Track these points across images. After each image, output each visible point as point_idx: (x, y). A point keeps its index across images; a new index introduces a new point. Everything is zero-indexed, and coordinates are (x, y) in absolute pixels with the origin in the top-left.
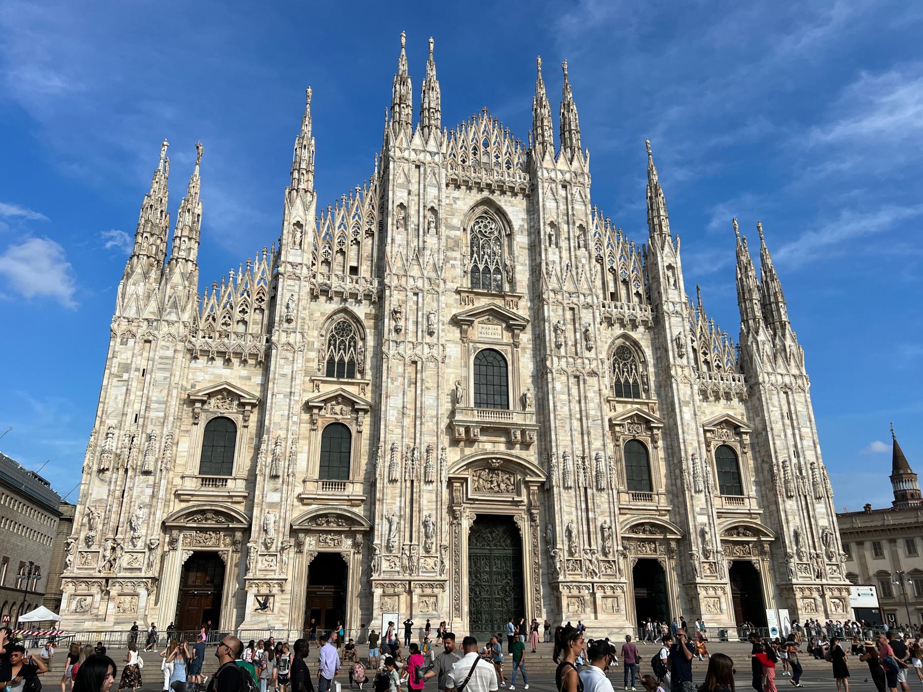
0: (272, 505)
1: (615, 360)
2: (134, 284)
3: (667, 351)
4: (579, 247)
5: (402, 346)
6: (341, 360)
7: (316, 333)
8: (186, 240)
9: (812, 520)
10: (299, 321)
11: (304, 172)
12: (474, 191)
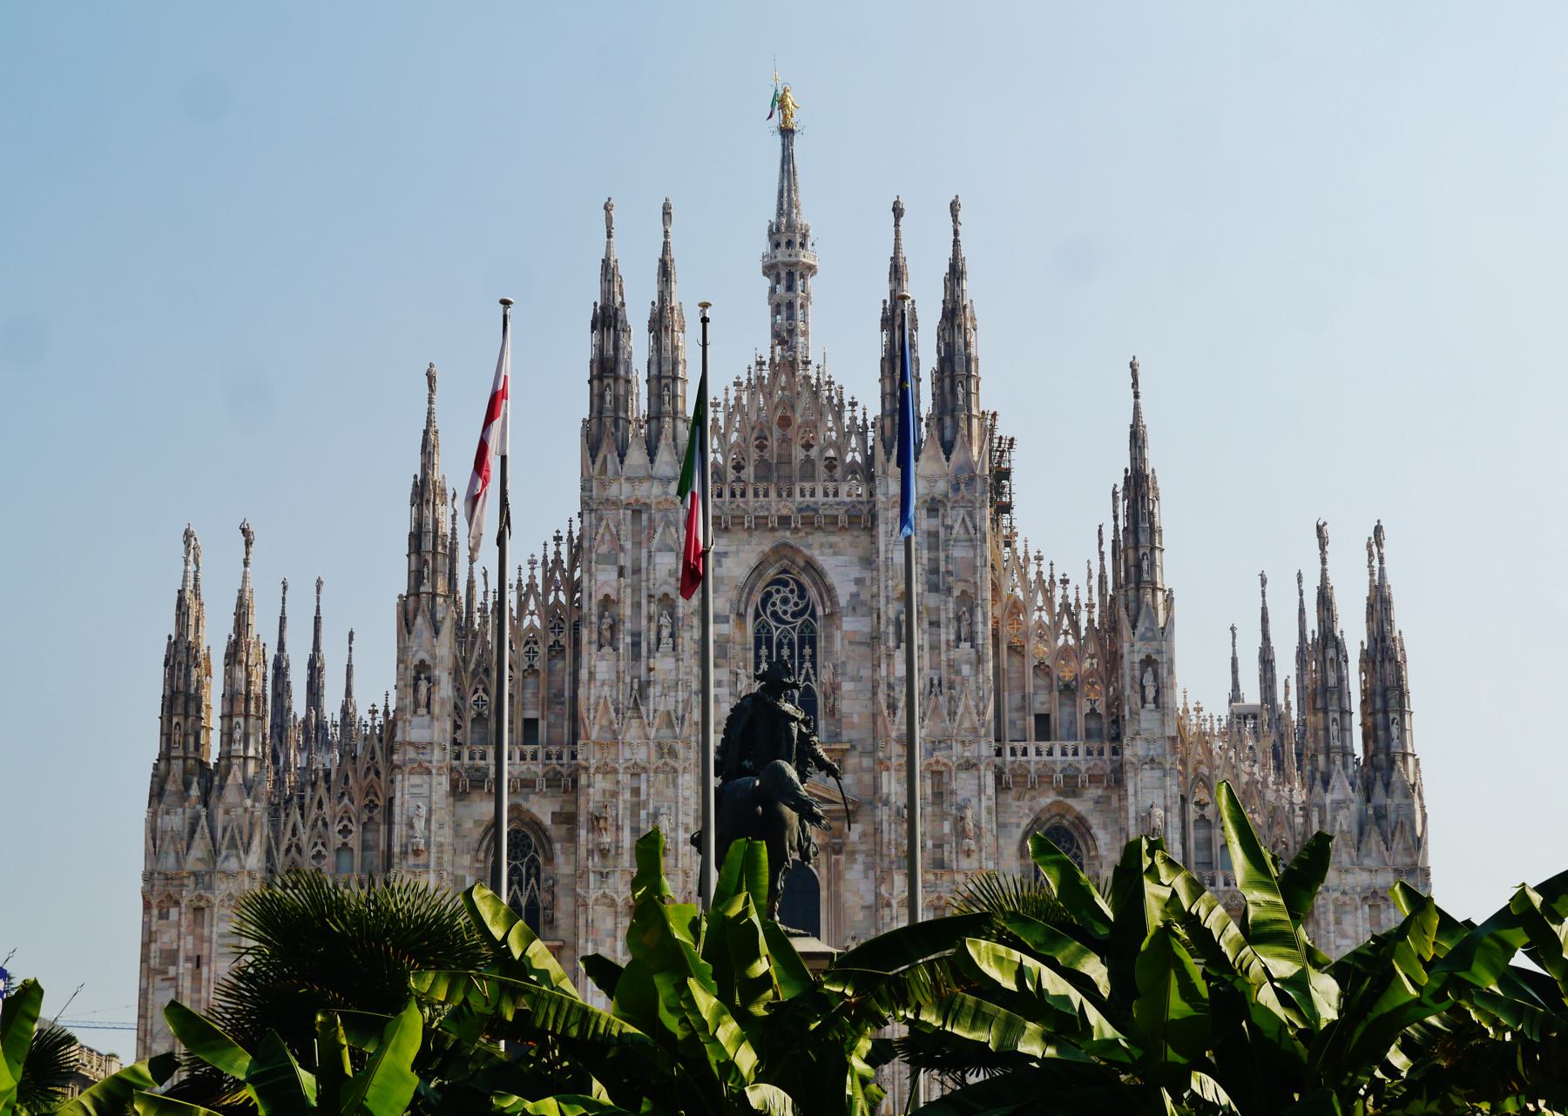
2: (168, 813)
4: (959, 638)
5: (611, 881)
7: (466, 860)
8: (241, 720)
10: (433, 850)
11: (429, 557)
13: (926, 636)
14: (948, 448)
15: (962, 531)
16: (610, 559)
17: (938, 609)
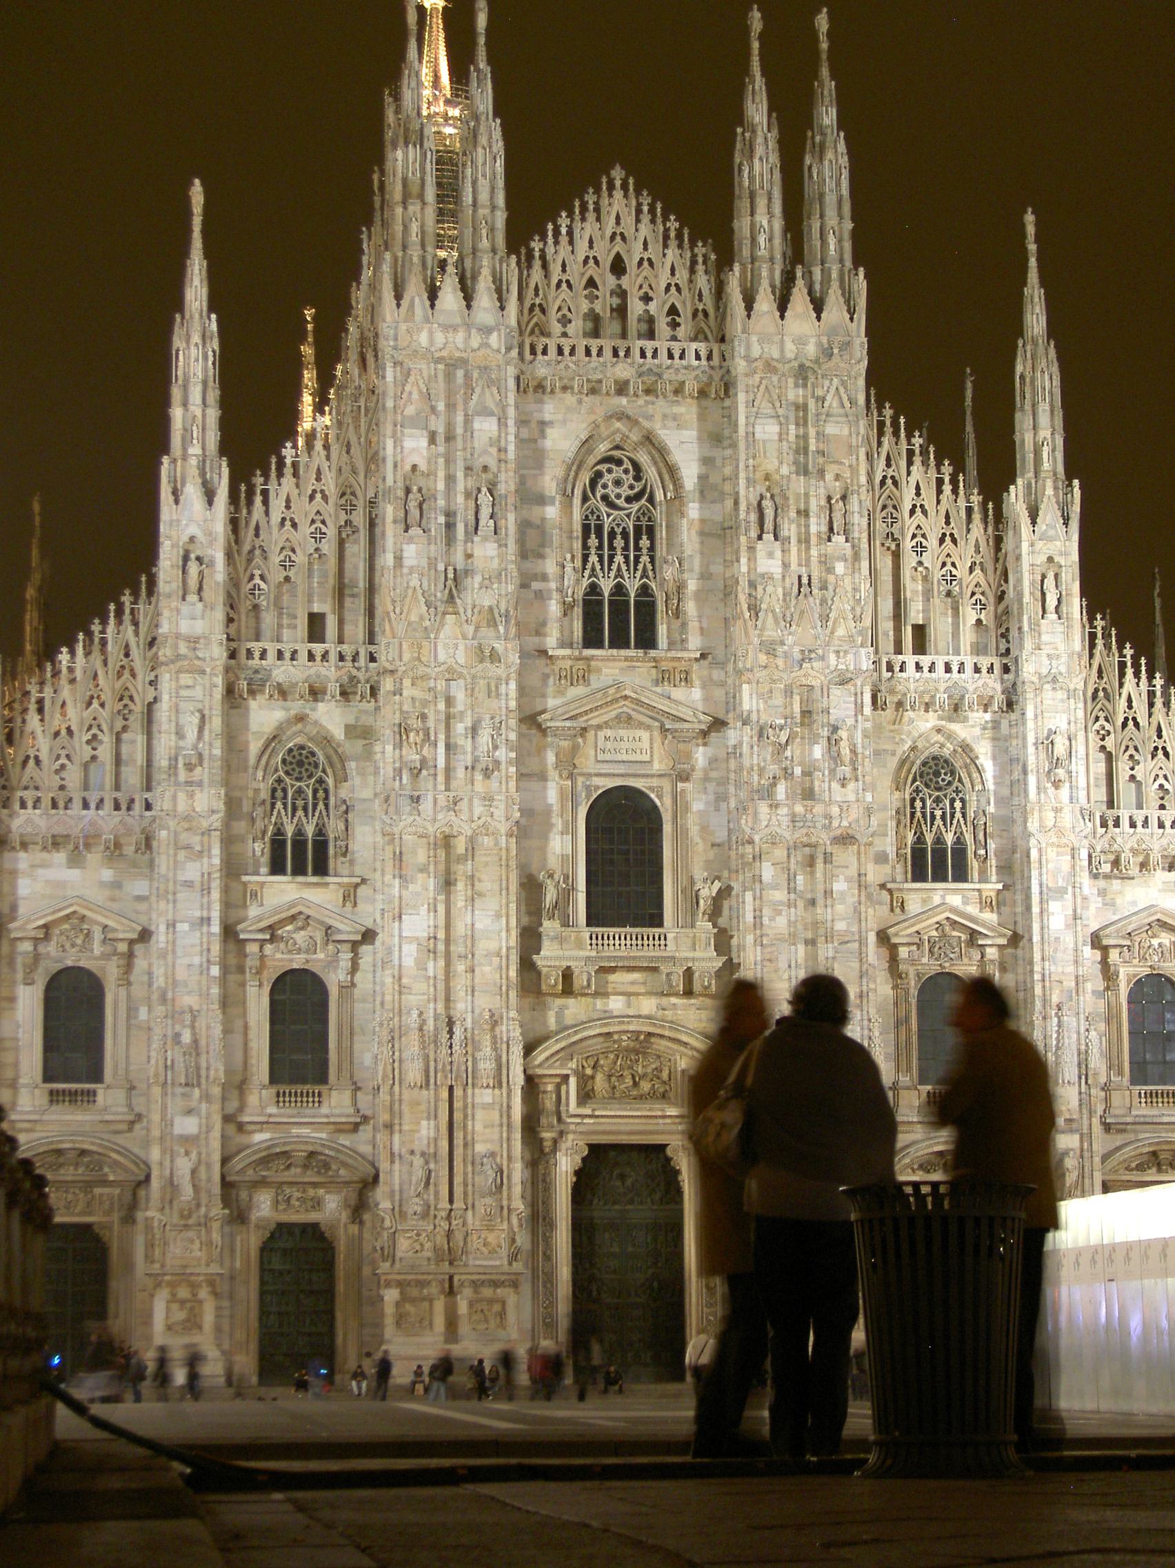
0: (186, 1140)
1: (917, 791)
3: (1025, 772)
4: (831, 529)
6: (299, 832)
12: (591, 397)
13: (793, 527)
14: (818, 306)
15: (835, 404)
16: (418, 421)
17: (807, 495)
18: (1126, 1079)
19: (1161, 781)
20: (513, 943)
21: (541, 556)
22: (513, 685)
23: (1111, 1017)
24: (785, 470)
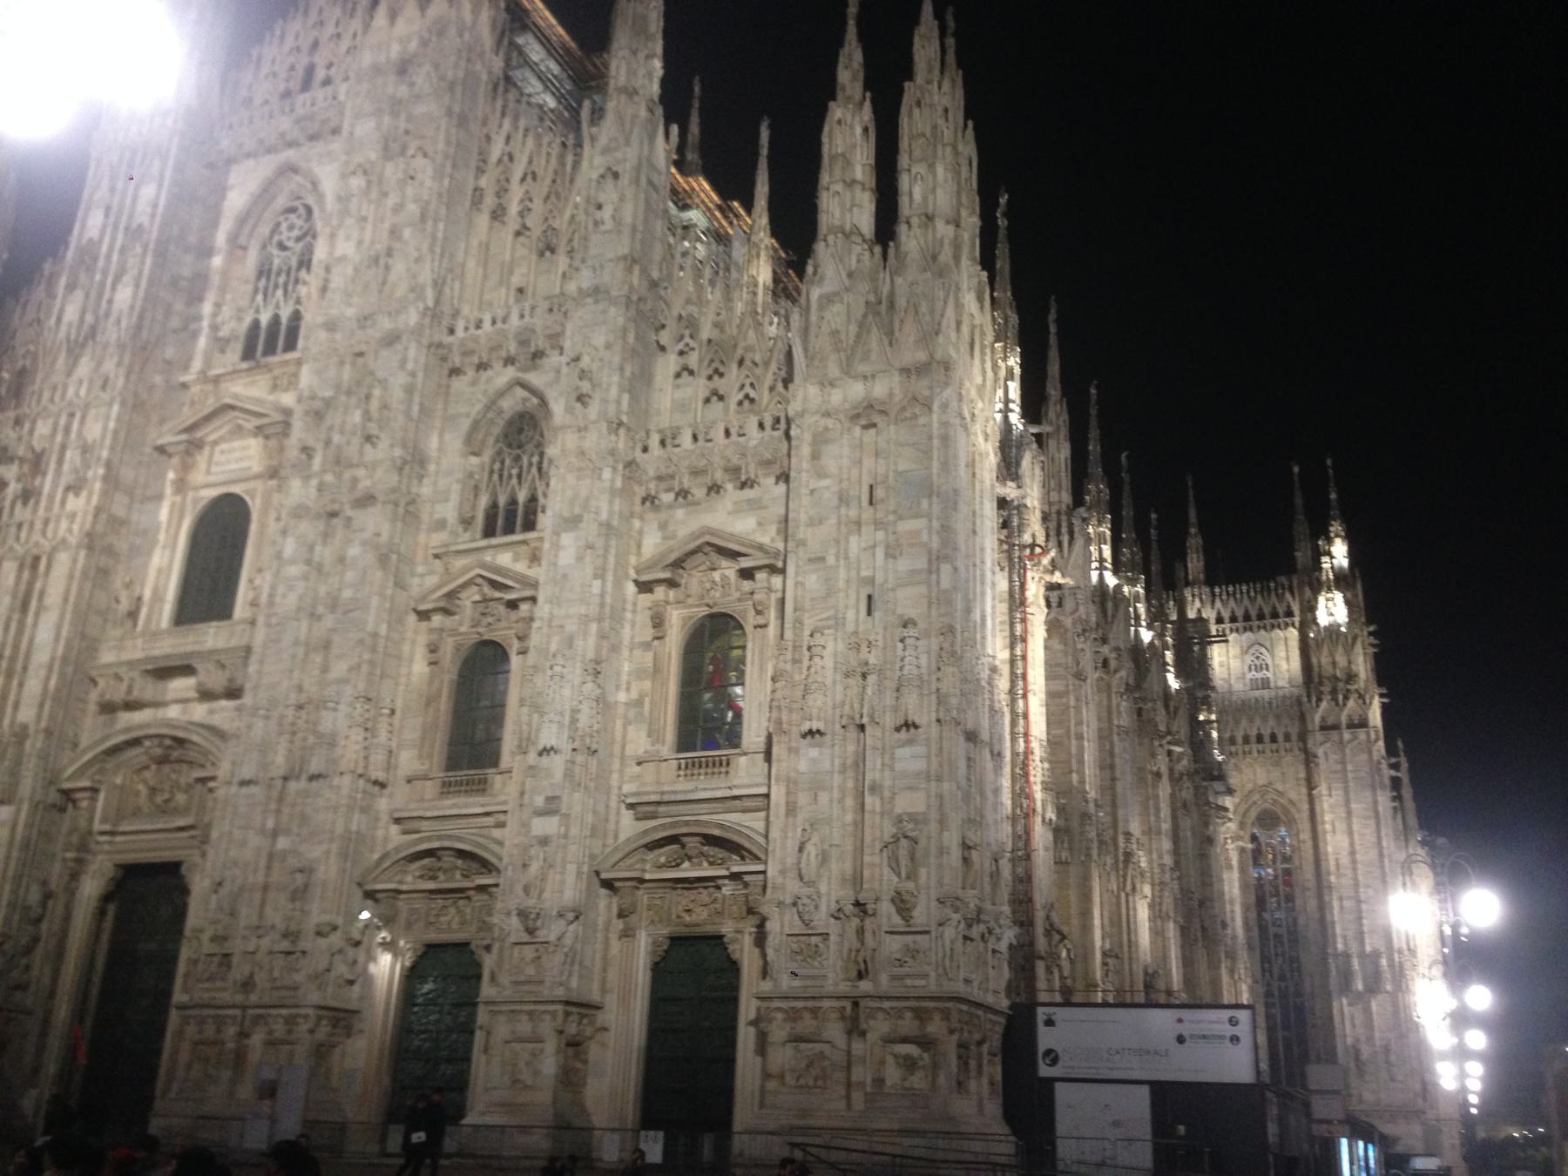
1: (499, 453)
9: (868, 799)
12: (268, 157)
13: (372, 207)
18: (667, 748)
19: (748, 389)
20: (60, 651)
21: (201, 299)
22: (116, 408)
23: (657, 670)
24: (373, 156)
